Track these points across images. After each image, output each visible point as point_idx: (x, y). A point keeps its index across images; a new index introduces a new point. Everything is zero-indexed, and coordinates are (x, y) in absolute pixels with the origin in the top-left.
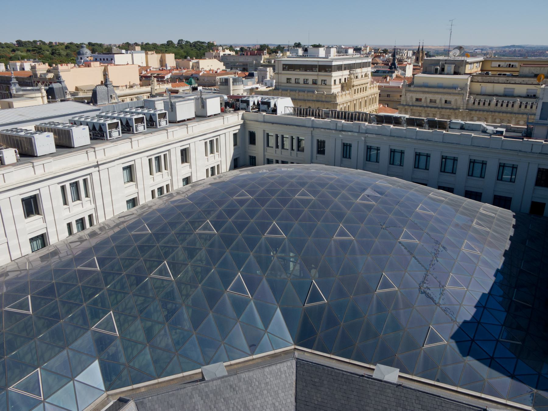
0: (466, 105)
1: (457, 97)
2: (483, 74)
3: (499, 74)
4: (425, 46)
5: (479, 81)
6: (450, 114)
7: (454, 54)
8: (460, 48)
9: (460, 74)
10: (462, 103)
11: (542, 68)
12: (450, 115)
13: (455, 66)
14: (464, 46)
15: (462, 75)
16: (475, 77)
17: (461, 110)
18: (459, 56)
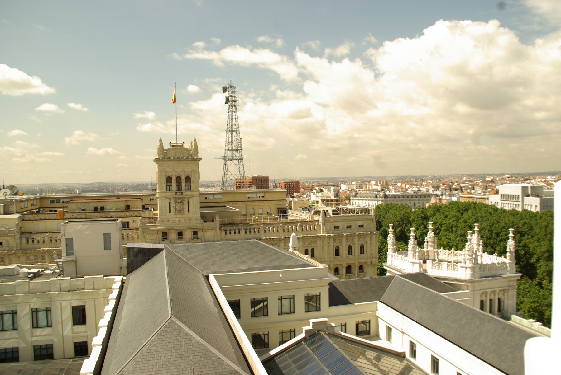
0: (19, 245)
1: (9, 238)
2: (34, 212)
3: (50, 211)
4: (6, 185)
5: (31, 219)
6: (3, 256)
7: (5, 194)
8: (12, 187)
9: (11, 214)
10: (15, 243)
11: (87, 204)
12: (3, 258)
13: (4, 206)
14: (16, 185)
15: (14, 214)
16: (25, 216)
17: (14, 251)
18: (10, 195)
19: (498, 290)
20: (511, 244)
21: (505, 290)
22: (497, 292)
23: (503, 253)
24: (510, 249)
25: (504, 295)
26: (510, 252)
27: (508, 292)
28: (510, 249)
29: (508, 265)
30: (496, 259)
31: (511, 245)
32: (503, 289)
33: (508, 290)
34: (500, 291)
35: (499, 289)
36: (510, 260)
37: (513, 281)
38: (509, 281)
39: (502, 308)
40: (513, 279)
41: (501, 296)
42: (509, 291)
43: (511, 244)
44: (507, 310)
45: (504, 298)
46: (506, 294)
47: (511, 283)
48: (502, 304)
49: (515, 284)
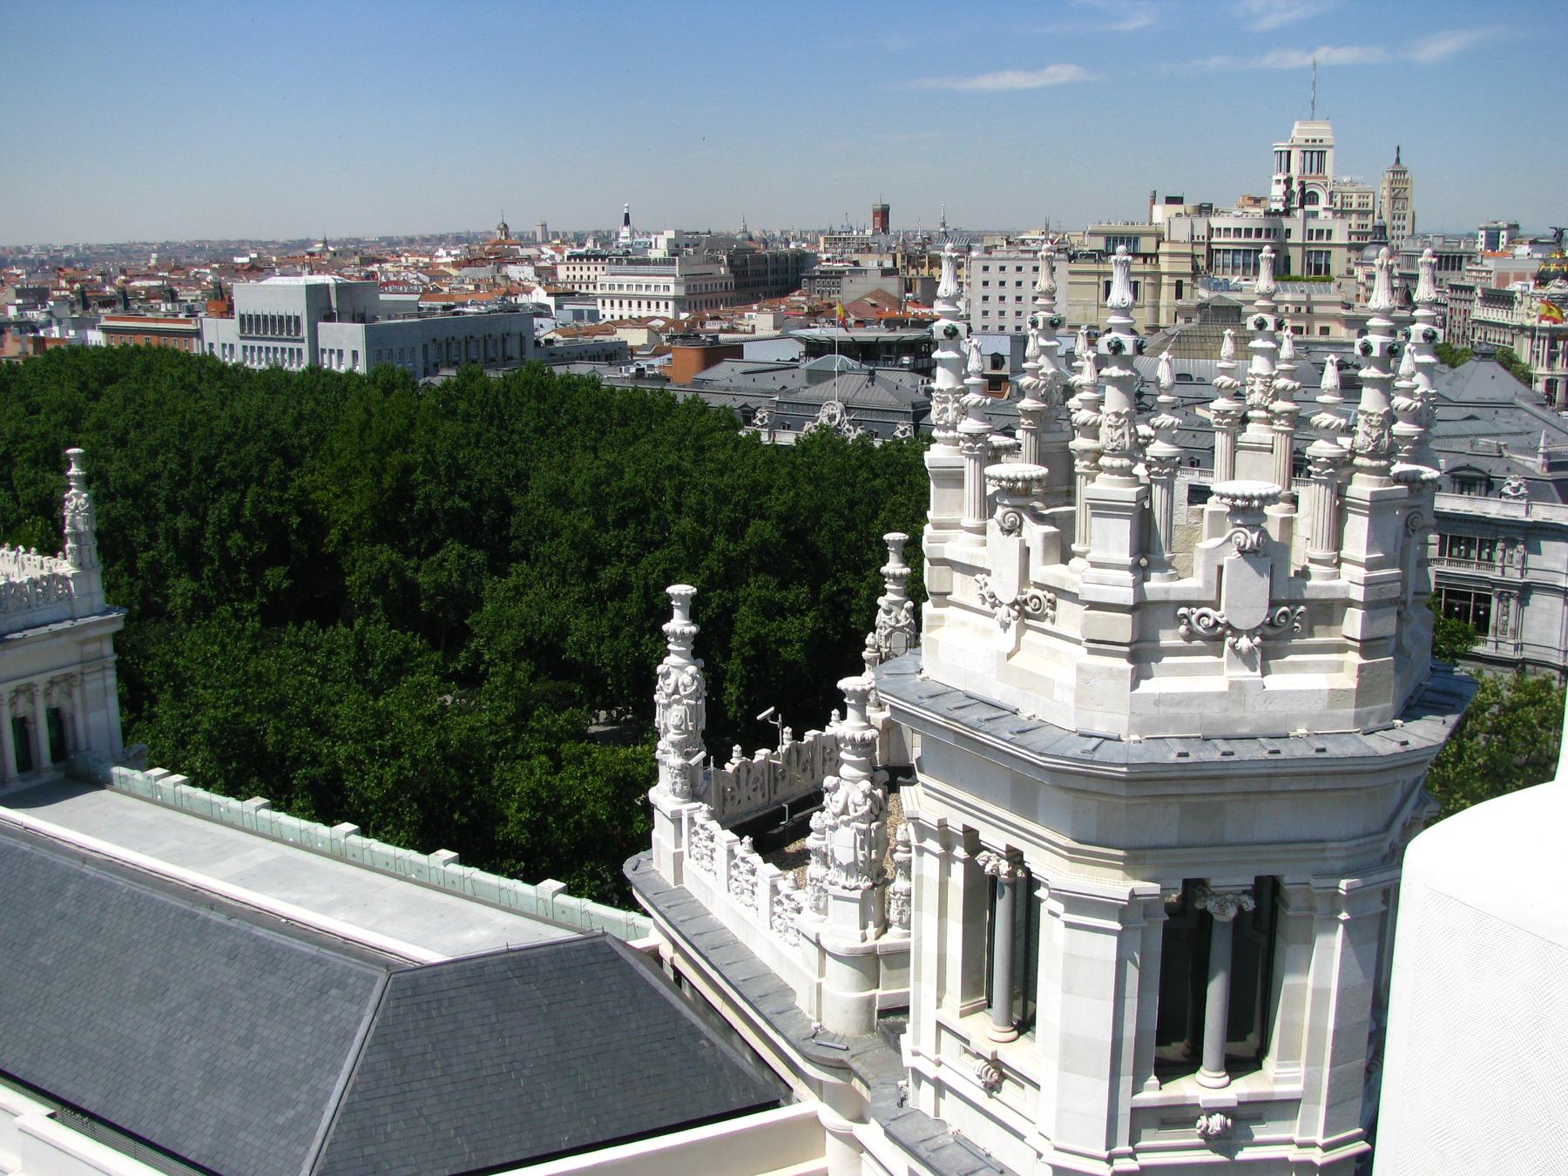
19: (41, 681)
20: (76, 503)
21: (72, 676)
22: (41, 688)
23: (51, 547)
24: (73, 525)
25: (70, 695)
26: (77, 536)
27: (82, 681)
28: (73, 525)
29: (72, 583)
30: (38, 566)
31: (77, 508)
32: (66, 675)
33: (82, 674)
34: (52, 682)
35: (48, 676)
36: (80, 565)
37: (100, 639)
38: (83, 643)
39: (70, 744)
40: (92, 633)
41: (57, 698)
42: (87, 678)
43: (76, 503)
44: (89, 749)
45: (74, 707)
46: (76, 692)
47: (92, 648)
48: (68, 726)
49: (108, 648)
